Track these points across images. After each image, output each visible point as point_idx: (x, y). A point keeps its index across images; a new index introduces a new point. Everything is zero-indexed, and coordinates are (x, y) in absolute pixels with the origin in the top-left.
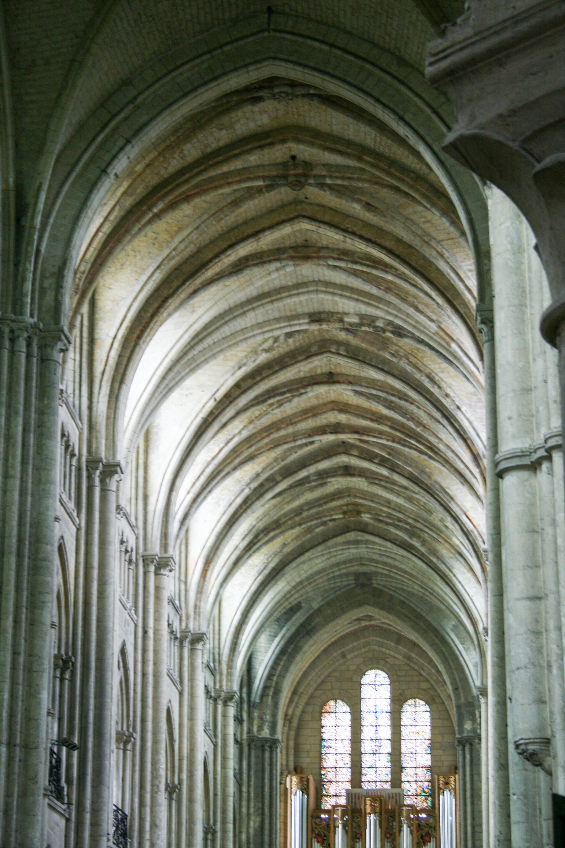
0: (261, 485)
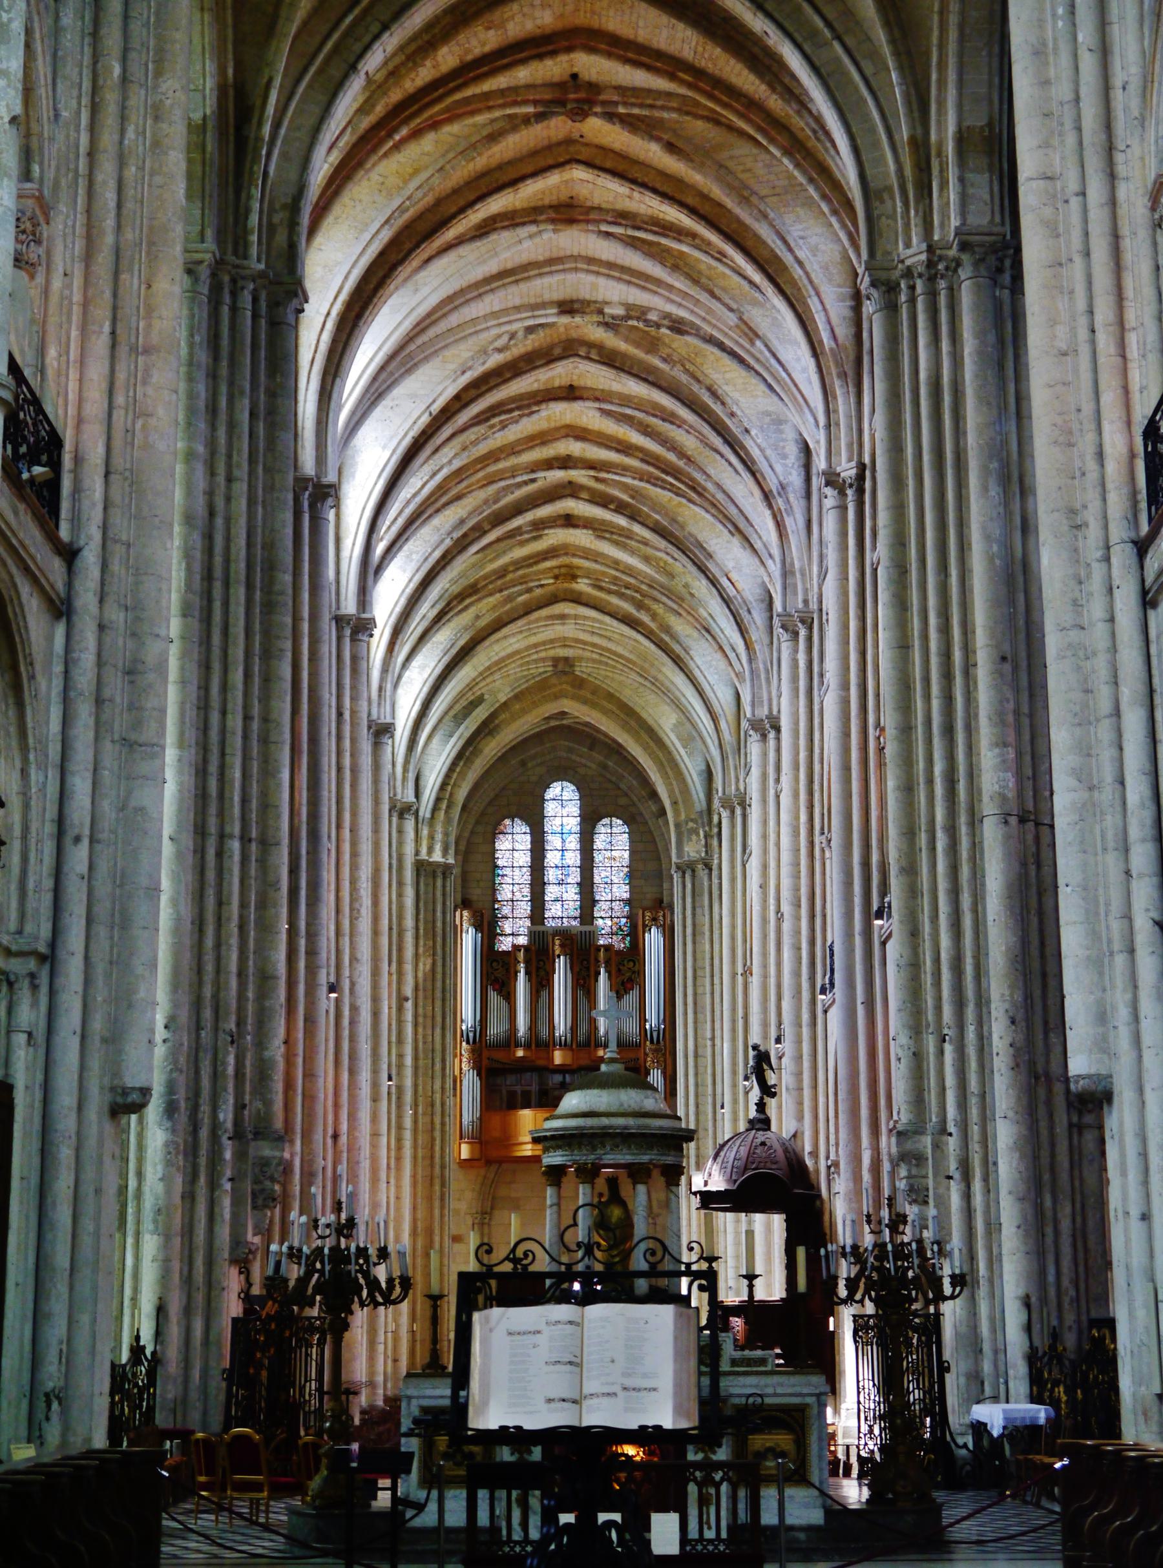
0: (465, 535)
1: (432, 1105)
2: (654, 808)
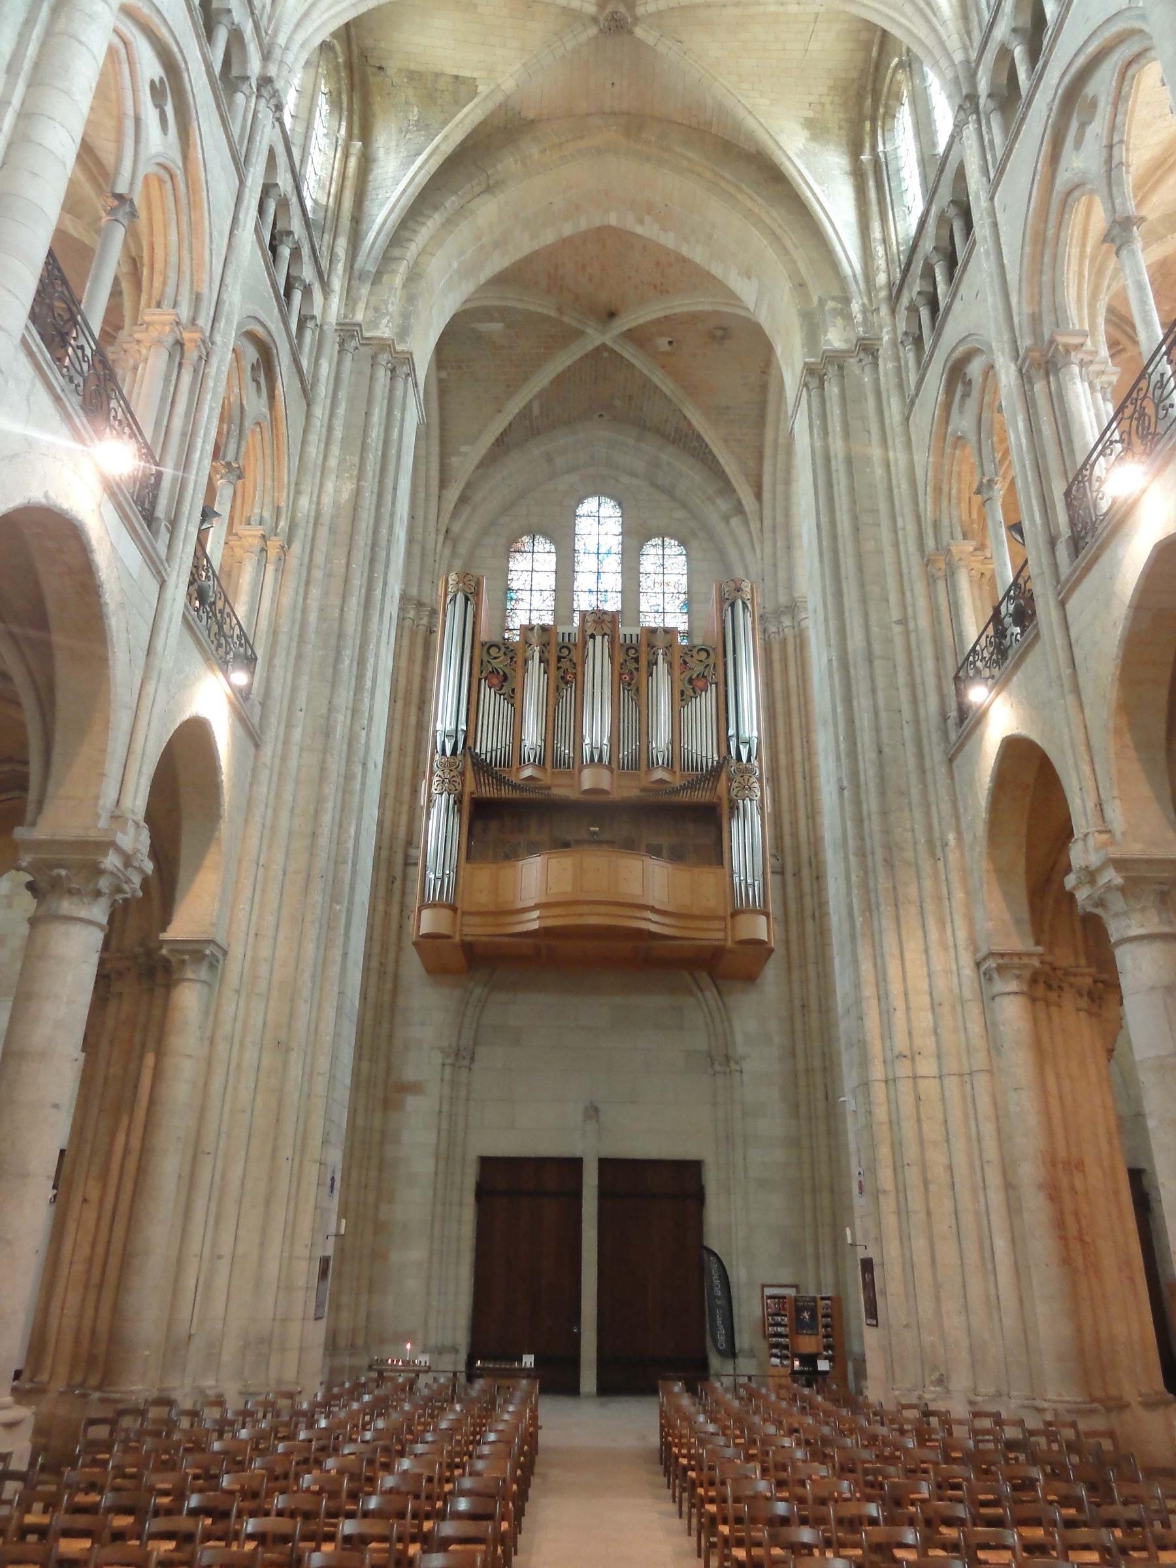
1: (328, 734)
2: (723, 505)
